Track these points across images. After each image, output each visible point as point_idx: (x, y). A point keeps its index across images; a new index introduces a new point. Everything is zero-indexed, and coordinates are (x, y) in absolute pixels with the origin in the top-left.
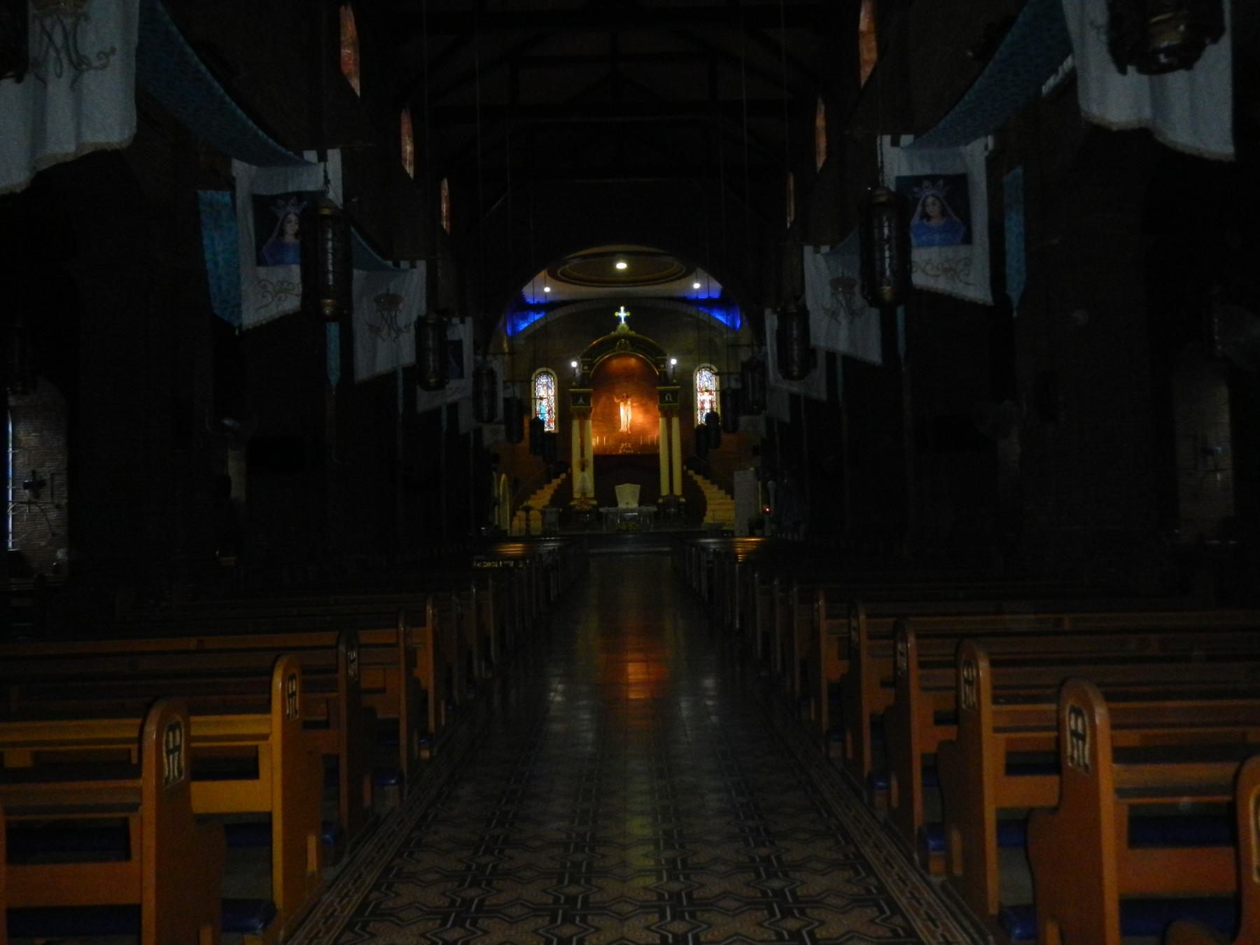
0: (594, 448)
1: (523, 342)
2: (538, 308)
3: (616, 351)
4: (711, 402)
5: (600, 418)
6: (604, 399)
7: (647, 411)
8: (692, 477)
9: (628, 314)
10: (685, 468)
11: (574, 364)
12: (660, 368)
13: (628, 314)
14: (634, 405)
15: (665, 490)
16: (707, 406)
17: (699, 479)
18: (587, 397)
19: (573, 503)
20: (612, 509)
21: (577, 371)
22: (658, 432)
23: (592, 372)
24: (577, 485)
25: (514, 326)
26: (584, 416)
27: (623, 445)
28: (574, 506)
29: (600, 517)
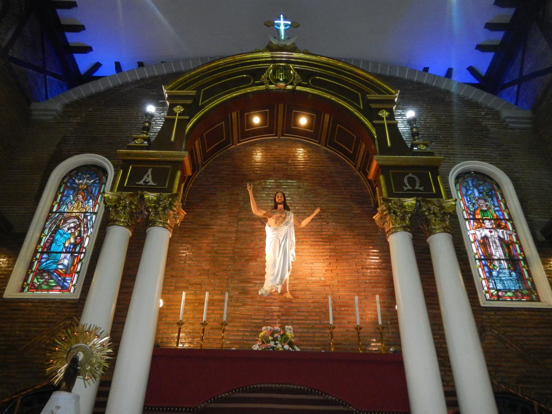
3: (262, 84)
4: (506, 245)
5: (206, 266)
14: (305, 223)
27: (265, 330)
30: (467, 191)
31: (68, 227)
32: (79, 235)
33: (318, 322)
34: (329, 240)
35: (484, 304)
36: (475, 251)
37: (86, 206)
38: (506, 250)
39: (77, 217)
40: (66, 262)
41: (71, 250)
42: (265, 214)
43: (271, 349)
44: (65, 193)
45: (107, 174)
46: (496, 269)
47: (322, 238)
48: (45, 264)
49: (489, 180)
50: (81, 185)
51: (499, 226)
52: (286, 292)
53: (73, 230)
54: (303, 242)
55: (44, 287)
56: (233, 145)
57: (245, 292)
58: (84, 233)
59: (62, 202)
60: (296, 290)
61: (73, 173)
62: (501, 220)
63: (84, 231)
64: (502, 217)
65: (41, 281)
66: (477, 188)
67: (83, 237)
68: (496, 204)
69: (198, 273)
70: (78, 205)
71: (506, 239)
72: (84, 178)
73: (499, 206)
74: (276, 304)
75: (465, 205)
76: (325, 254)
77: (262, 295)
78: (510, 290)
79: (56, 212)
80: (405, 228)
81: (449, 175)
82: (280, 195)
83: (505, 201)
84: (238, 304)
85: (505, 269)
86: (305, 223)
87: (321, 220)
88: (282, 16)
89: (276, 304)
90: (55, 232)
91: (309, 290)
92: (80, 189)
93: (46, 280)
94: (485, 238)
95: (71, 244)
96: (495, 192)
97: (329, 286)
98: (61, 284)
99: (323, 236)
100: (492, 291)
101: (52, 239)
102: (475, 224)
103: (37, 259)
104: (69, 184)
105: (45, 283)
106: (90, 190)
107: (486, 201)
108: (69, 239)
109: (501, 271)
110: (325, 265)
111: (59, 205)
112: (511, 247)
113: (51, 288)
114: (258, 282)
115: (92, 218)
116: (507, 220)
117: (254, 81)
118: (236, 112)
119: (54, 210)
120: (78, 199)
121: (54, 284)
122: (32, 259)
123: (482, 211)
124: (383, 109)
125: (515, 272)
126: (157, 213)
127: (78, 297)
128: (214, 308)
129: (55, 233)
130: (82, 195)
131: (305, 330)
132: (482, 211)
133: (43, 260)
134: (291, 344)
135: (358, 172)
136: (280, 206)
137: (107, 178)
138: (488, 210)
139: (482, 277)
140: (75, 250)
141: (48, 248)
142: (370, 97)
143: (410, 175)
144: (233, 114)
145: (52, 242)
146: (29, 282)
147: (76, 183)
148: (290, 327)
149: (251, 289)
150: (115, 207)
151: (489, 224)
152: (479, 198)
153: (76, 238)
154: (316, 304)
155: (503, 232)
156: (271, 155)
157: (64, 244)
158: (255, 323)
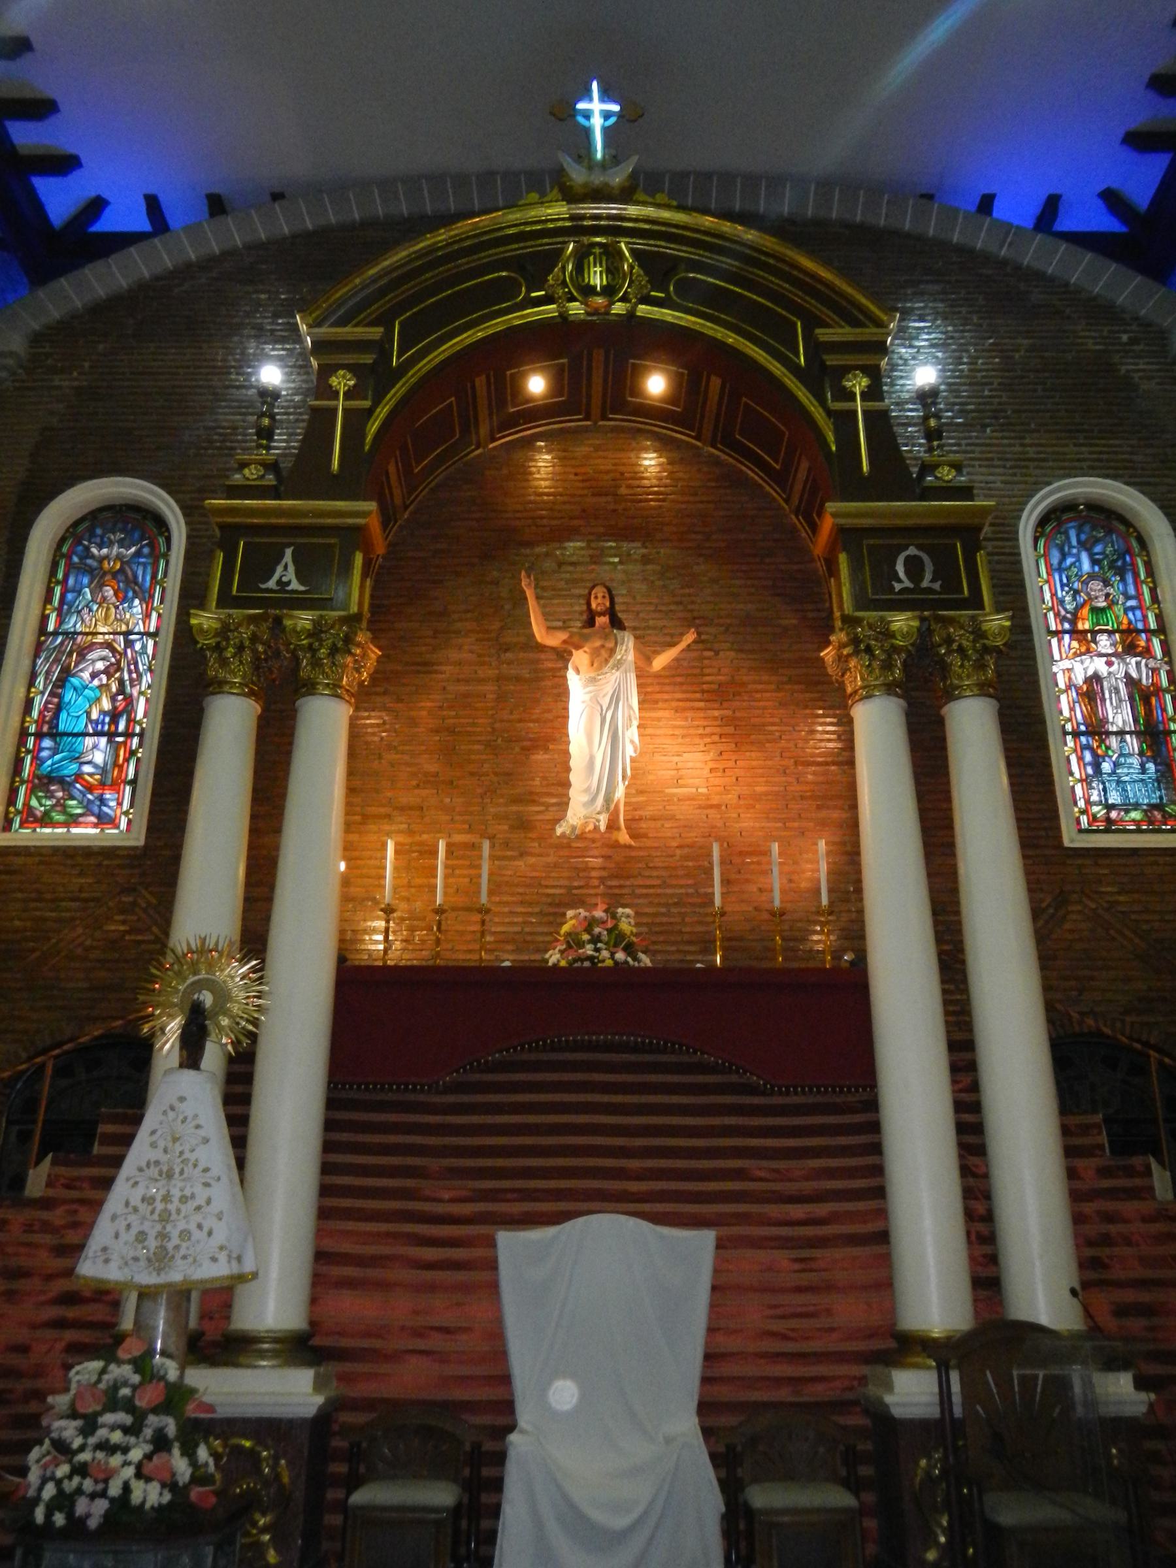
3: (548, 300)
5: (431, 766)
14: (661, 661)
23: (382, 412)
27: (573, 919)
30: (1064, 557)
31: (91, 670)
32: (121, 690)
33: (691, 891)
34: (720, 695)
35: (1072, 841)
36: (1066, 713)
37: (128, 616)
38: (1141, 709)
39: (109, 645)
40: (99, 758)
41: (106, 727)
42: (565, 642)
43: (587, 964)
44: (71, 582)
45: (168, 530)
46: (1111, 757)
47: (703, 692)
48: (49, 762)
49: (1122, 528)
50: (106, 562)
51: (1130, 649)
52: (618, 829)
53: (104, 677)
54: (656, 702)
55: (58, 817)
56: (477, 448)
57: (523, 825)
58: (132, 686)
59: (65, 607)
60: (641, 819)
61: (80, 529)
62: (1139, 632)
63: (131, 680)
64: (1140, 626)
65: (49, 803)
66: (1089, 551)
67: (131, 696)
68: (1132, 591)
69: (414, 783)
70: (106, 614)
71: (1144, 682)
72: (110, 544)
73: (1139, 596)
74: (596, 853)
75: (1054, 595)
76: (708, 730)
77: (563, 835)
78: (1136, 806)
79: (55, 633)
80: (890, 689)
81: (1019, 518)
82: (600, 591)
83: (1154, 582)
84: (509, 853)
85: (1130, 755)
86: (661, 661)
87: (701, 646)
88: (595, 85)
89: (596, 853)
90: (62, 682)
91: (672, 818)
92: (105, 573)
93: (58, 800)
94: (1096, 678)
95: (103, 713)
96: (1131, 558)
97: (718, 806)
98: (96, 809)
99: (705, 687)
100: (1095, 809)
101: (56, 700)
102: (1075, 644)
103: (28, 752)
104: (75, 559)
105: (58, 808)
106: (130, 573)
107: (1106, 583)
108: (98, 700)
109: (1122, 760)
110: (709, 758)
111: (59, 615)
112: (1153, 700)
113: (74, 821)
114: (554, 800)
115: (144, 647)
116: (1154, 632)
117: (529, 291)
118: (484, 377)
119: (51, 627)
120: (104, 599)
121: (79, 811)
122: (18, 751)
123: (1096, 611)
124: (857, 367)
125: (1156, 764)
126: (316, 663)
127: (141, 842)
128: (455, 862)
129: (63, 687)
130: (113, 588)
131: (663, 910)
132: (1096, 611)
133: (44, 754)
134: (629, 949)
135: (793, 517)
136: (602, 620)
137: (168, 540)
138: (1110, 607)
139: (1077, 775)
140: (117, 728)
141: (50, 722)
142: (824, 334)
143: (912, 551)
144: (477, 381)
145: (59, 709)
146: (20, 805)
147: (93, 557)
148: (628, 911)
149: (540, 817)
150: (218, 648)
151: (1108, 643)
152: (1092, 576)
153: (113, 699)
154: (686, 850)
155: (1138, 664)
156: (576, 474)
157: (88, 713)
158: (548, 895)
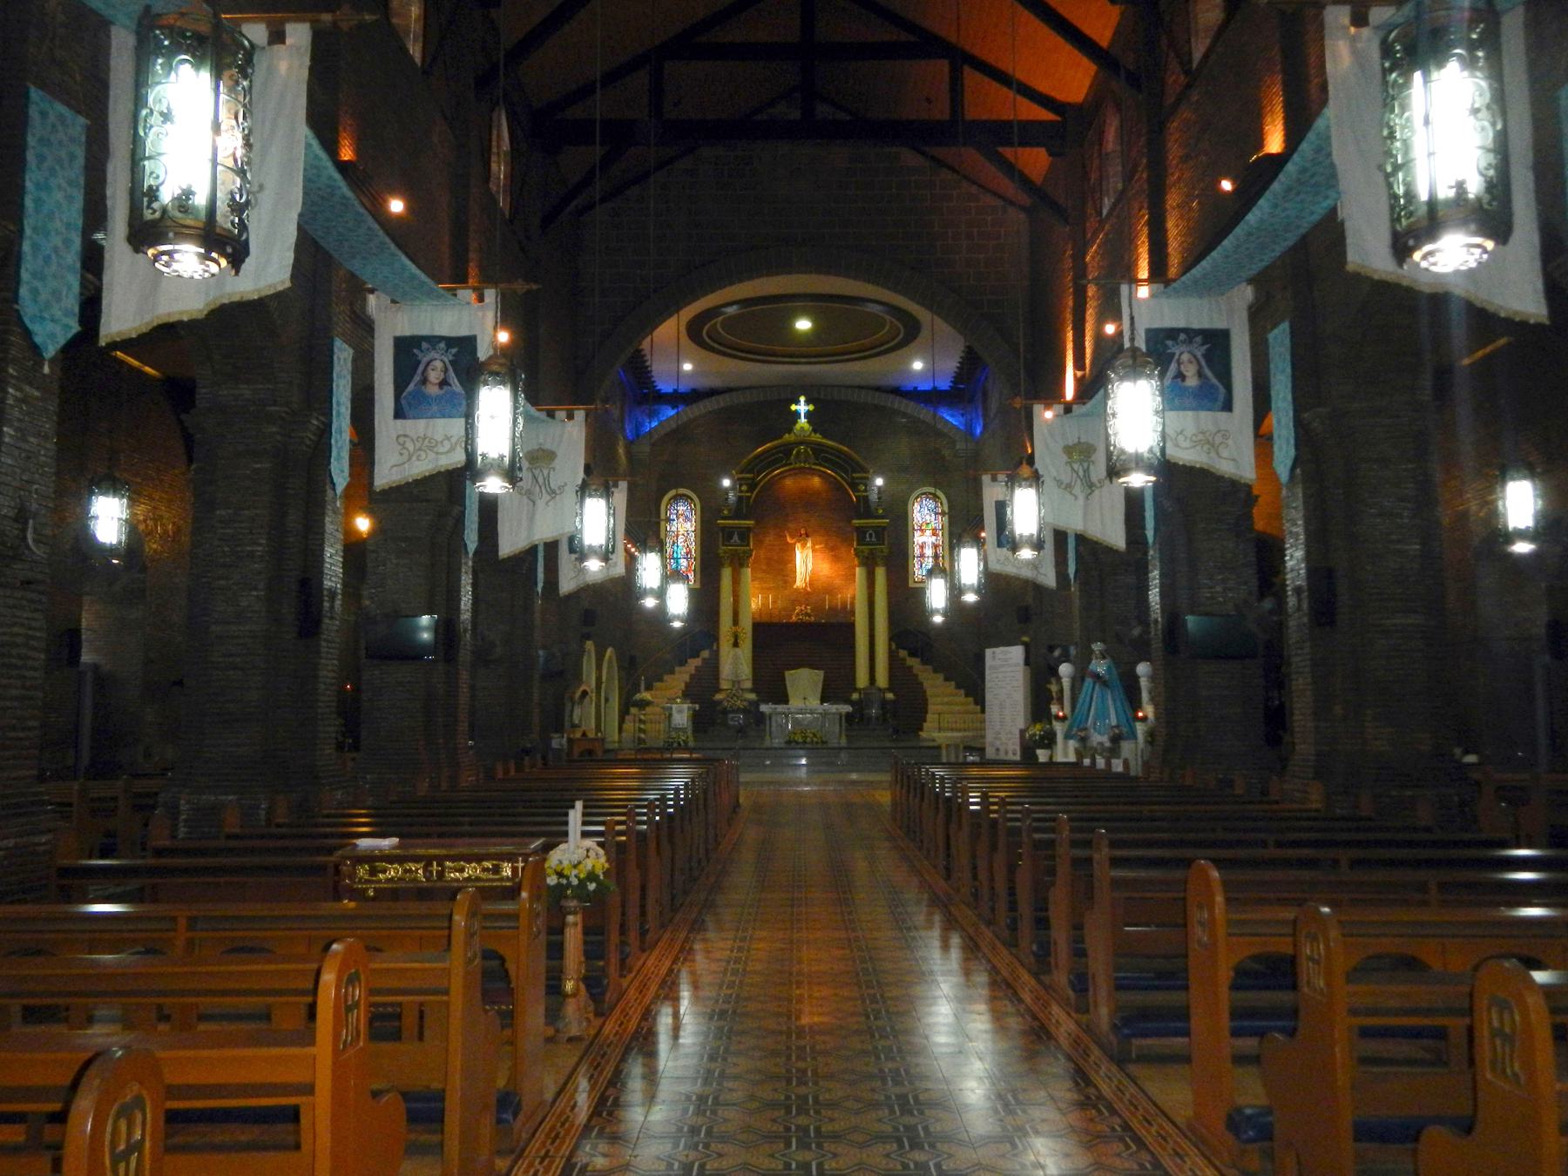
0: (753, 614)
1: (647, 449)
2: (676, 399)
3: (791, 464)
4: (935, 546)
5: (764, 568)
6: (770, 539)
7: (836, 559)
8: (904, 659)
9: (811, 407)
10: (894, 646)
11: (726, 483)
12: (859, 491)
13: (811, 407)
15: (862, 680)
16: (929, 552)
17: (914, 663)
18: (744, 534)
19: (719, 697)
20: (780, 708)
21: (731, 495)
22: (854, 591)
23: (753, 496)
24: (726, 670)
25: (639, 425)
26: (739, 562)
28: (720, 702)
29: (761, 719)
34: (832, 549)
51: (934, 535)
